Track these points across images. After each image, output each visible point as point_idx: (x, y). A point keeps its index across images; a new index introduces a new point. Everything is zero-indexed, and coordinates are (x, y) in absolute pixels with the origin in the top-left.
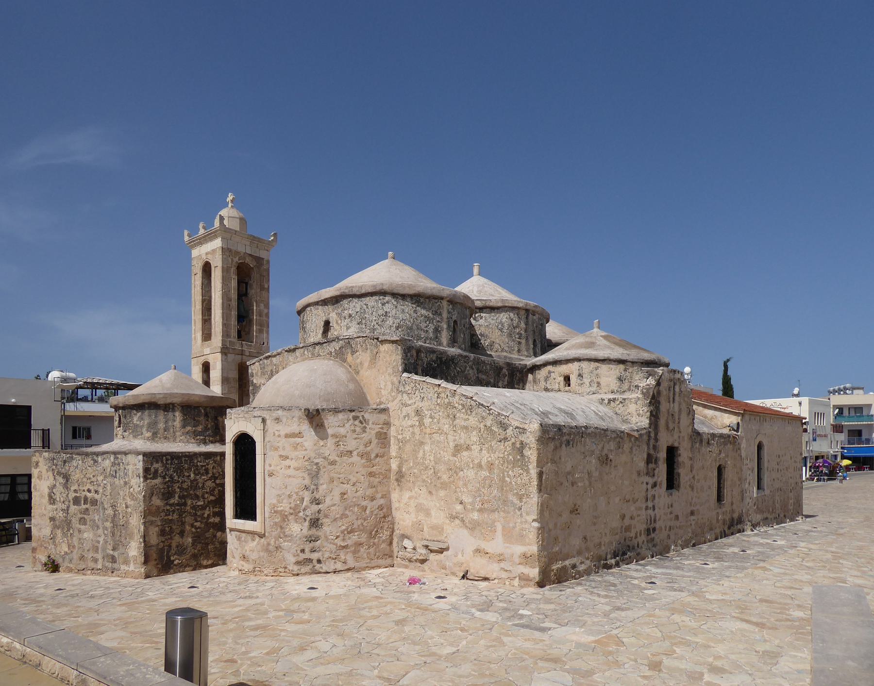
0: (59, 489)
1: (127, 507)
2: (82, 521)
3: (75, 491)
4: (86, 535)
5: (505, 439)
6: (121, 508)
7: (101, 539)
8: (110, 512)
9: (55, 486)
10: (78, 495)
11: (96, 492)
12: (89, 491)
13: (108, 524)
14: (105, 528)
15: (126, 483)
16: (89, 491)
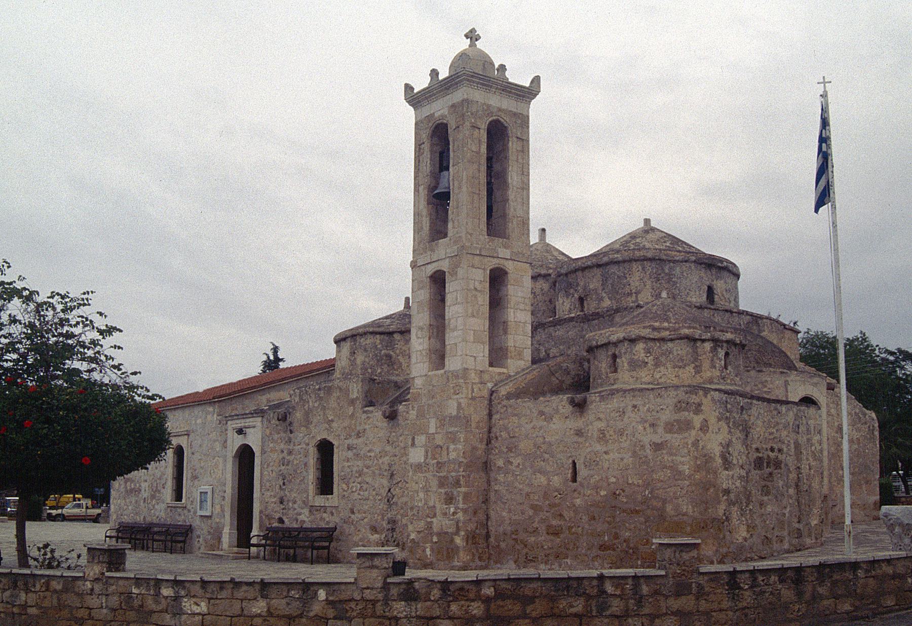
0: (738, 447)
1: (810, 469)
2: (766, 491)
3: (757, 450)
4: (769, 509)
5: (866, 423)
6: (805, 470)
7: (787, 511)
8: (793, 476)
9: (730, 441)
10: (761, 455)
11: (780, 450)
12: (772, 450)
13: (792, 491)
14: (790, 497)
15: (808, 440)
16: (772, 450)
